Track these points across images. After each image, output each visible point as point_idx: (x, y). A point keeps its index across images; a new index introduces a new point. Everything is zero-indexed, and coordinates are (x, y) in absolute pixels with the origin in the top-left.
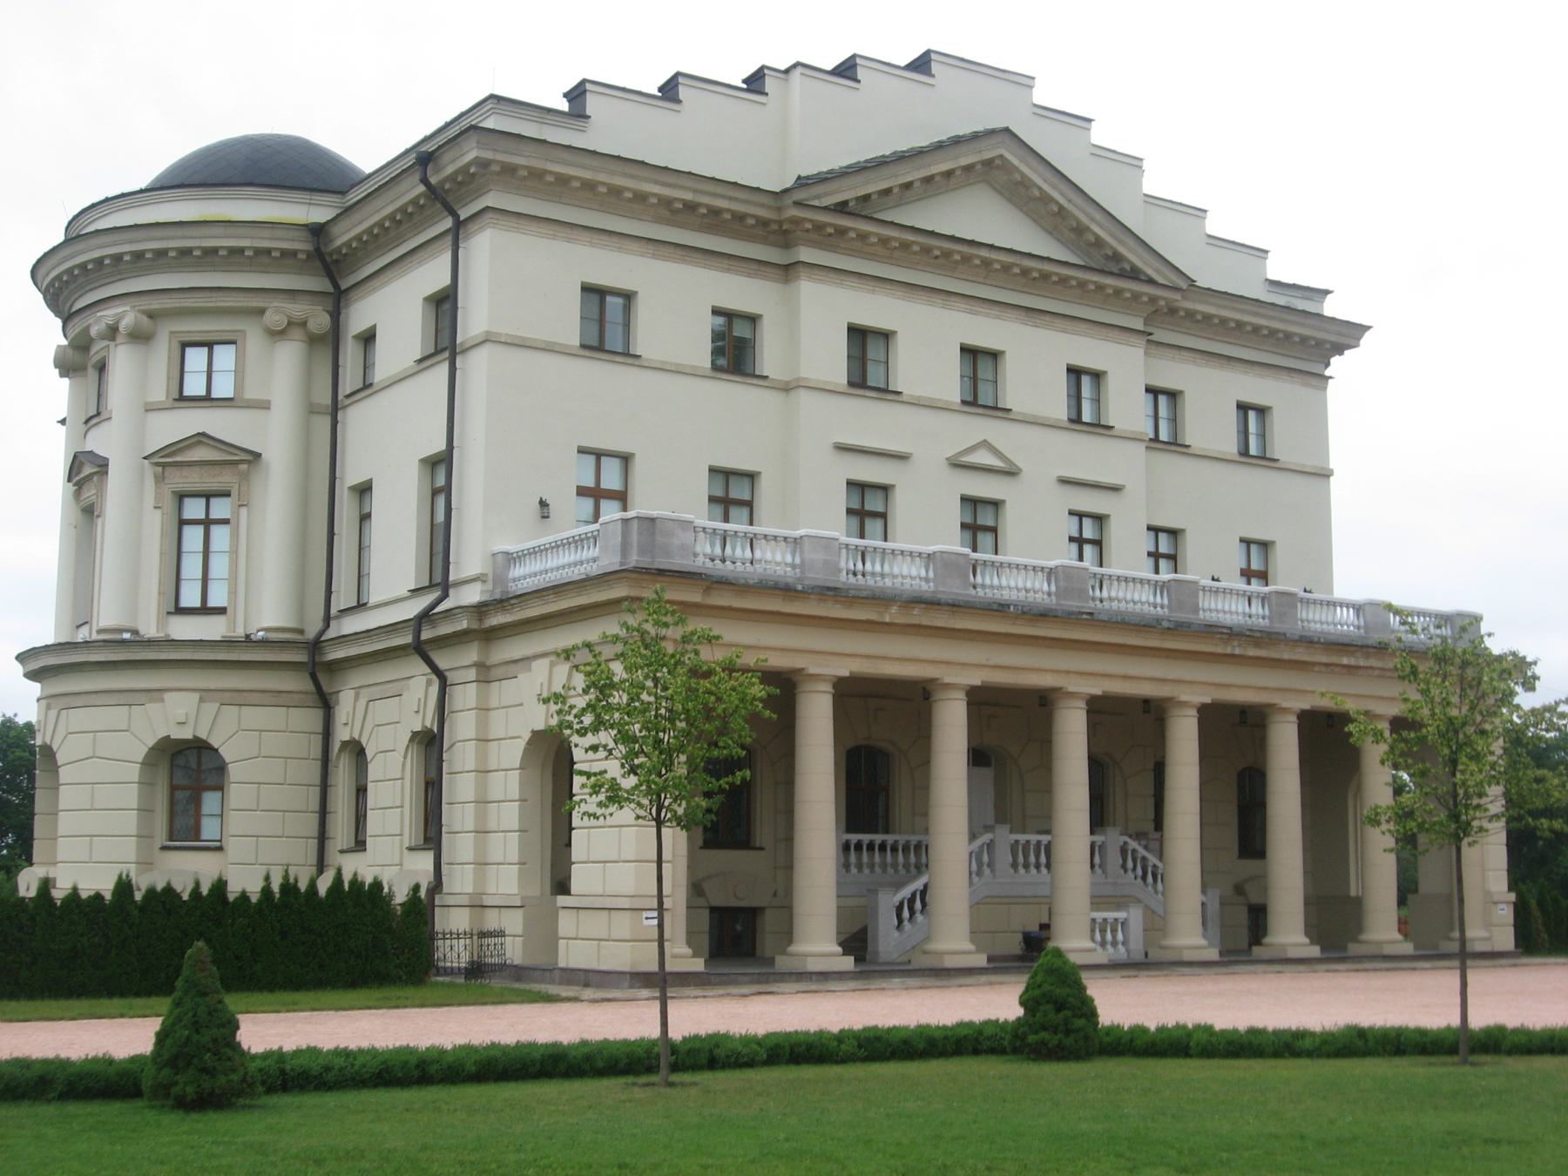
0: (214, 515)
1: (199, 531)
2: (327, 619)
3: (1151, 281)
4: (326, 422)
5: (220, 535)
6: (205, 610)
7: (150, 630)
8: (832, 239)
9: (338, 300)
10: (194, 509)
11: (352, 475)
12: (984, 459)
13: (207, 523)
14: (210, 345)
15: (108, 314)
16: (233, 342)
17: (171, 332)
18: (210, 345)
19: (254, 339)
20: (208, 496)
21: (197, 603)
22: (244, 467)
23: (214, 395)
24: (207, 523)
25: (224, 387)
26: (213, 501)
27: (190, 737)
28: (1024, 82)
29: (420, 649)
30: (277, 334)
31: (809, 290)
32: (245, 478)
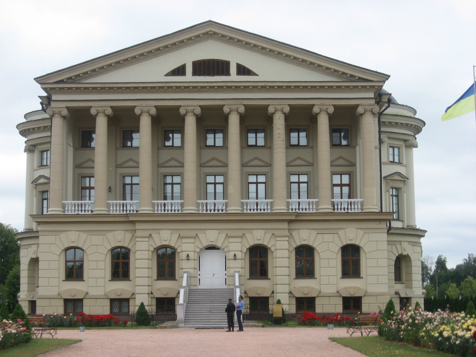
13: (392, 196)
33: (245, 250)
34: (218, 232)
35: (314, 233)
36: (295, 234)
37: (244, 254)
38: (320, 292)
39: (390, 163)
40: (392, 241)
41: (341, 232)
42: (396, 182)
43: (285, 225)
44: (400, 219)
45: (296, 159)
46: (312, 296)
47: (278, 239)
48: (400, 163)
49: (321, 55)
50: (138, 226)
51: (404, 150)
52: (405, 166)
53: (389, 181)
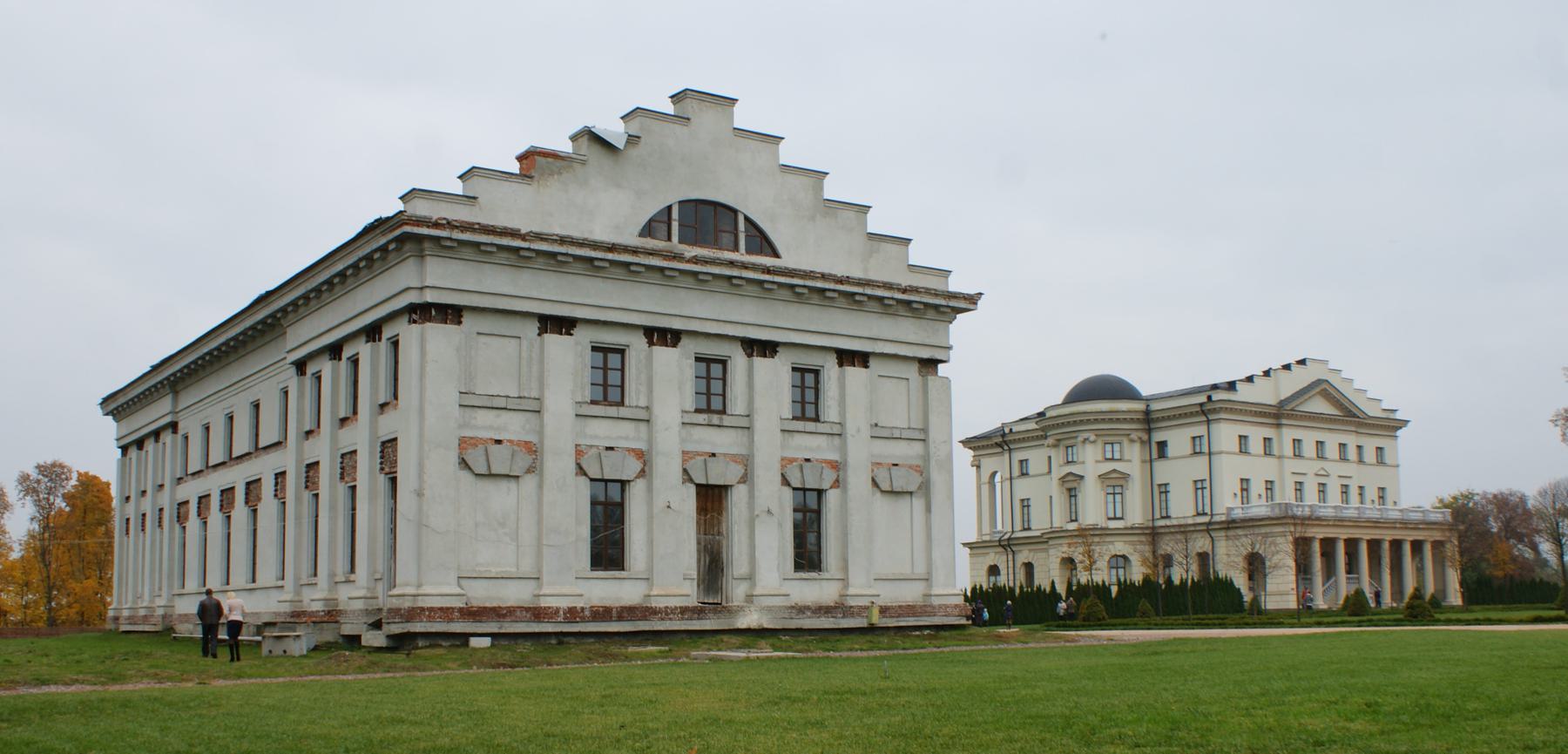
1: (1112, 496)
2: (1153, 520)
3: (1358, 417)
4: (1148, 465)
5: (1118, 498)
6: (1115, 518)
7: (1104, 525)
8: (1289, 417)
9: (1149, 431)
11: (1158, 480)
12: (1322, 472)
13: (1114, 494)
14: (1112, 444)
15: (1086, 435)
18: (1112, 444)
19: (1125, 441)
20: (1114, 486)
21: (1112, 516)
24: (1114, 494)
25: (1117, 456)
28: (1325, 362)
29: (1208, 531)
30: (1132, 441)
31: (1285, 430)
32: (1127, 481)
48: (1120, 460)
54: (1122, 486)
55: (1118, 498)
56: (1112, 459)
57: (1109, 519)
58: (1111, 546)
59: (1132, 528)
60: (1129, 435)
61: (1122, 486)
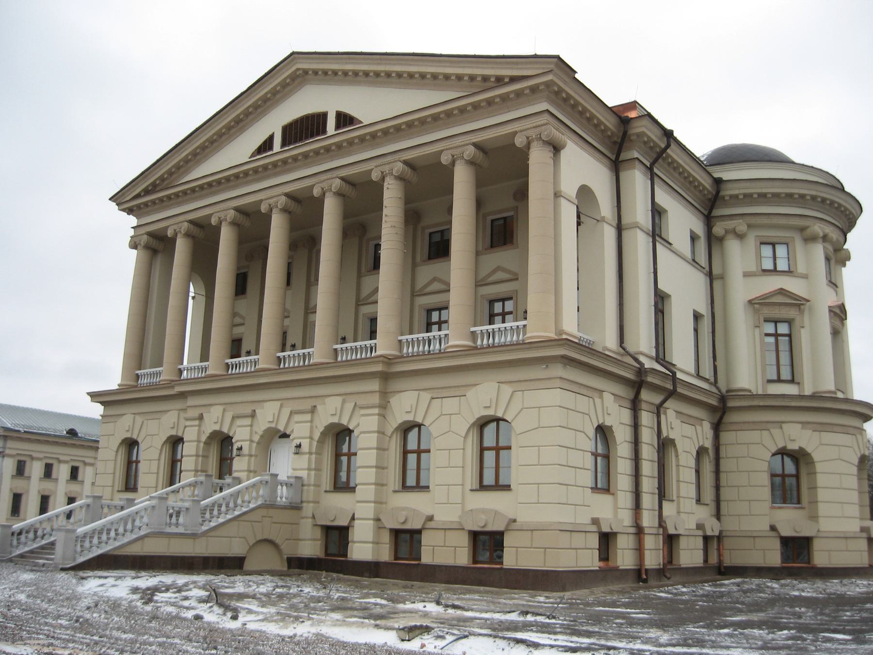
0: (779, 332)
1: (772, 340)
6: (779, 380)
7: (760, 392)
10: (770, 328)
13: (776, 335)
14: (773, 245)
16: (787, 244)
17: (756, 236)
18: (773, 245)
21: (775, 377)
22: (802, 307)
23: (778, 270)
25: (782, 265)
26: (778, 324)
27: (797, 448)
30: (810, 239)
32: (801, 312)
33: (317, 435)
34: (278, 404)
35: (426, 396)
36: (394, 401)
37: (315, 443)
38: (430, 518)
39: (761, 273)
40: (761, 422)
41: (471, 393)
42: (777, 307)
43: (374, 385)
44: (796, 380)
45: (494, 271)
46: (412, 528)
47: (363, 412)
48: (789, 272)
49: (441, 56)
50: (191, 401)
51: (799, 246)
52: (805, 277)
53: (756, 306)
54: (790, 322)
55: (784, 341)
56: (775, 271)
57: (770, 381)
58: (776, 432)
59: (814, 397)
60: (802, 229)
61: (790, 322)
